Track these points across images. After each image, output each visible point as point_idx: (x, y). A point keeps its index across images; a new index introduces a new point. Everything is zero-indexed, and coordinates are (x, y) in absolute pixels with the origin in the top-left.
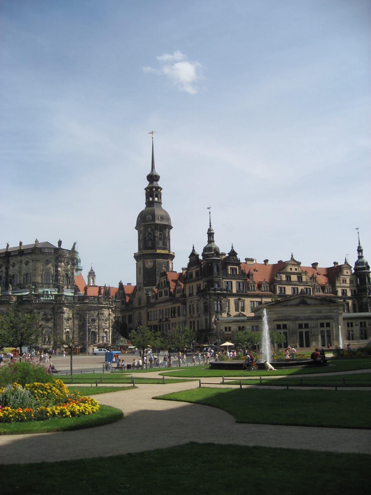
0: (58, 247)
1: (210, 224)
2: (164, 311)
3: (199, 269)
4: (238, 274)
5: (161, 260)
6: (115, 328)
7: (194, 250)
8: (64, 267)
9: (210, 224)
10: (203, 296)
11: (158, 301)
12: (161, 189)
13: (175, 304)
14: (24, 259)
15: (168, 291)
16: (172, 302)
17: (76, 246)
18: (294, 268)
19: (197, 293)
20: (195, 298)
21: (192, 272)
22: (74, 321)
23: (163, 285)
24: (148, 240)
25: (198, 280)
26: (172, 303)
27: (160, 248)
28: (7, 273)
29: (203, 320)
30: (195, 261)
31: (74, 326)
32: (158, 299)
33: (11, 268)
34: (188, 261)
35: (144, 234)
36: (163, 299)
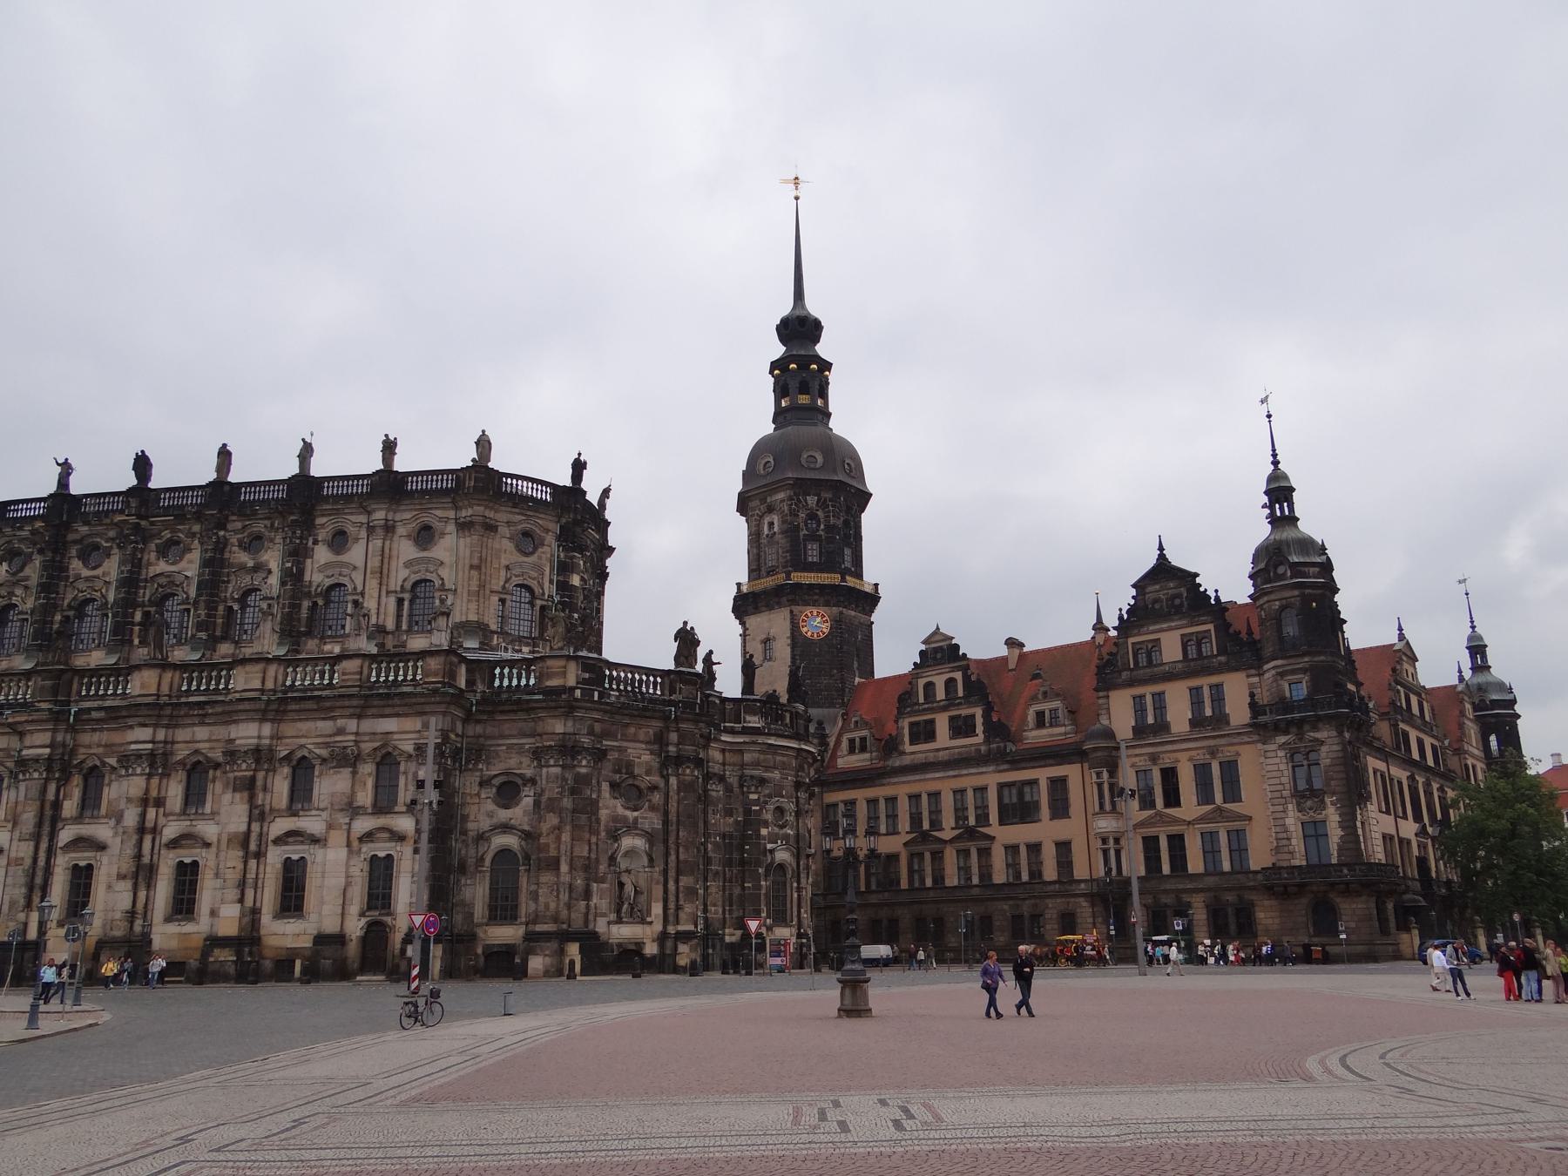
0: (568, 483)
1: (1274, 455)
2: (947, 802)
3: (1211, 627)
7: (1162, 557)
9: (1274, 455)
10: (1278, 728)
11: (896, 762)
14: (407, 518)
15: (979, 721)
17: (608, 502)
19: (1197, 722)
22: (705, 812)
23: (940, 694)
26: (1005, 767)
28: (293, 577)
29: (1292, 828)
30: (1179, 596)
32: (904, 753)
33: (322, 554)
35: (794, 514)
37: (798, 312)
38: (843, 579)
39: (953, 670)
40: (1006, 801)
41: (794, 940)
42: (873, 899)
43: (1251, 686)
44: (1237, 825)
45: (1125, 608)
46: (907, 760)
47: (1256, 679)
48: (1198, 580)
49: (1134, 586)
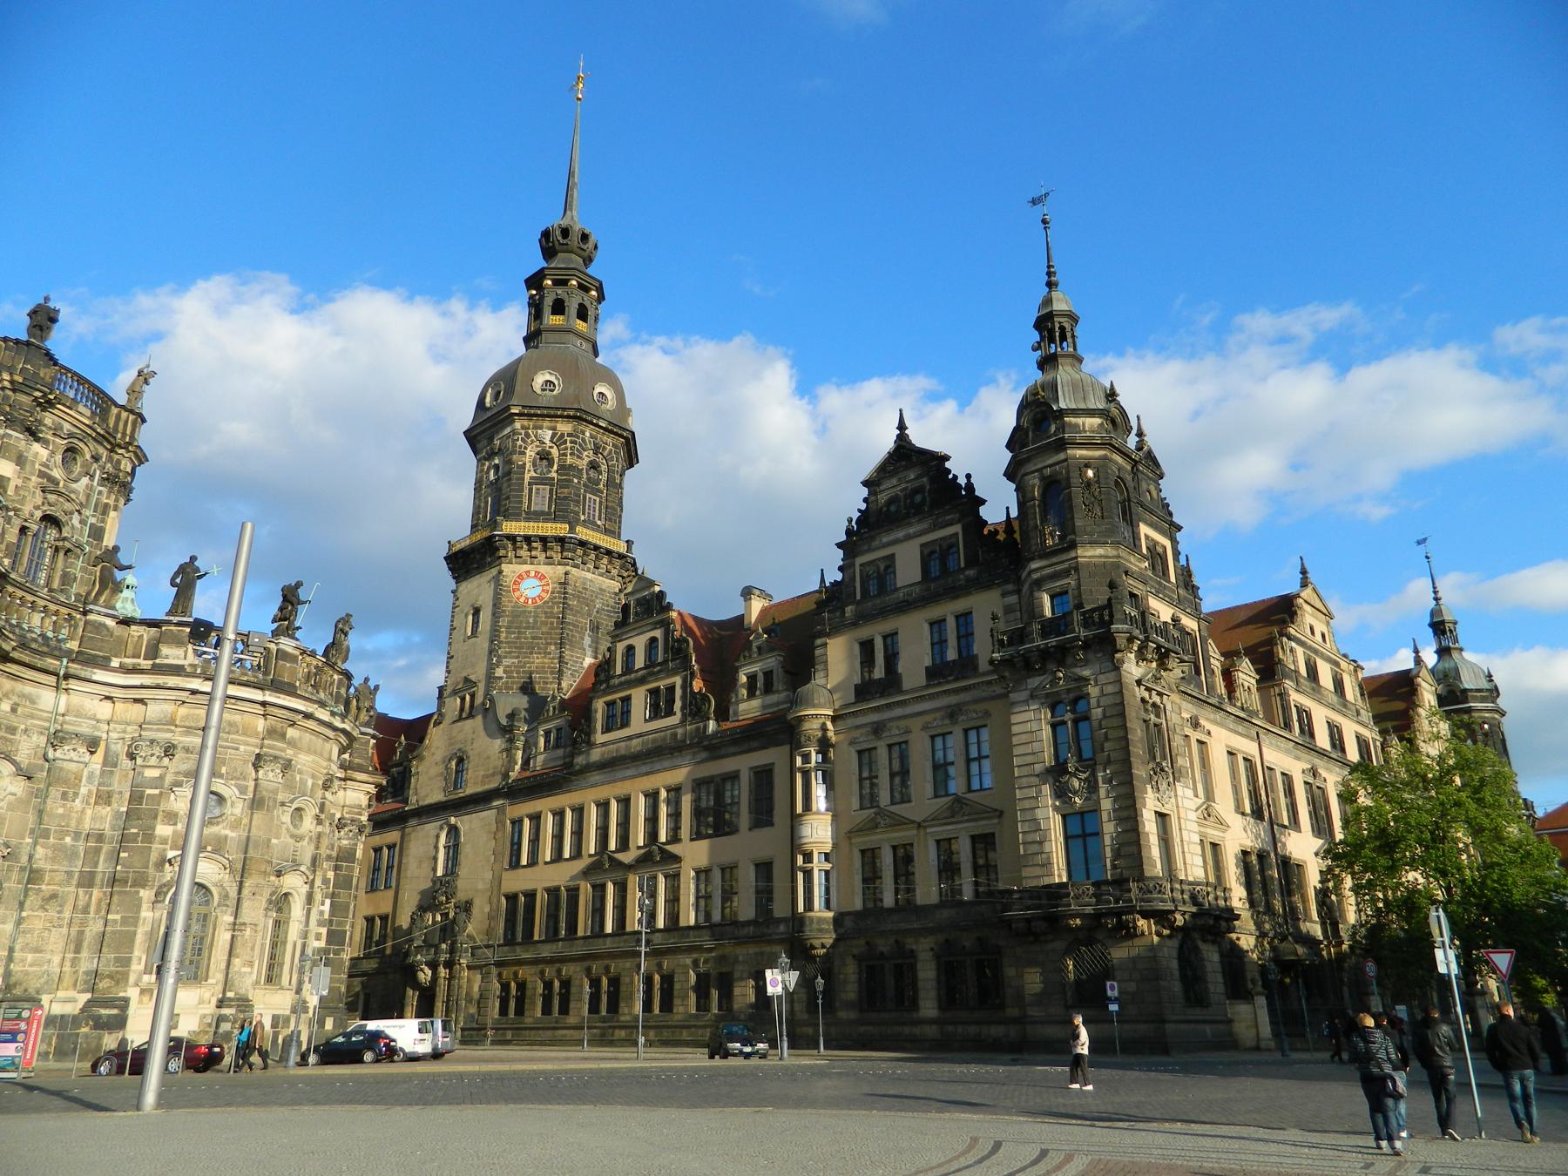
3: (957, 528)
4: (1173, 579)
5: (589, 576)
6: (333, 896)
8: (42, 475)
12: (601, 298)
13: (734, 754)
15: (678, 692)
16: (706, 748)
18: (1320, 627)
19: (936, 673)
20: (921, 698)
21: (891, 558)
22: (43, 795)
23: (640, 661)
24: (535, 481)
25: (954, 592)
26: (704, 755)
27: (589, 524)
30: (916, 491)
31: (40, 834)
34: (854, 501)
36: (635, 742)
37: (564, 223)
38: (572, 530)
39: (655, 626)
40: (704, 804)
41: (210, 1009)
42: (546, 951)
43: (1008, 610)
44: (982, 827)
45: (855, 515)
46: (596, 755)
47: (1013, 599)
48: (947, 464)
49: (866, 483)
